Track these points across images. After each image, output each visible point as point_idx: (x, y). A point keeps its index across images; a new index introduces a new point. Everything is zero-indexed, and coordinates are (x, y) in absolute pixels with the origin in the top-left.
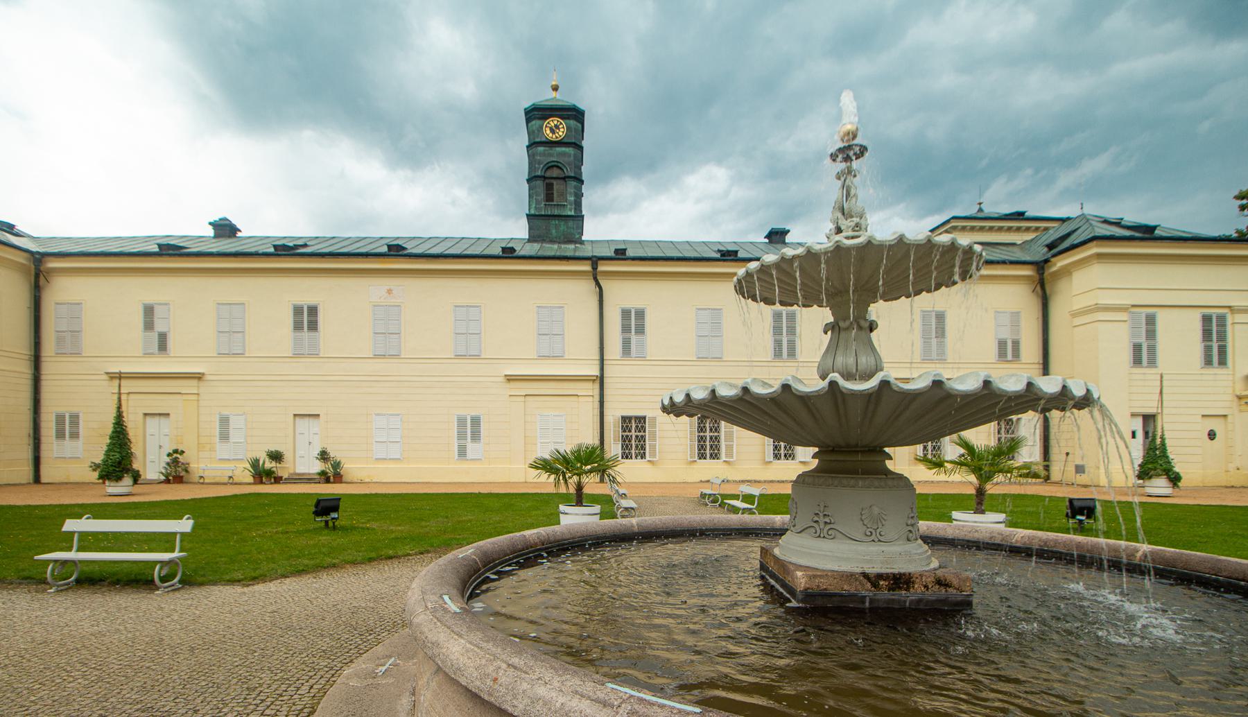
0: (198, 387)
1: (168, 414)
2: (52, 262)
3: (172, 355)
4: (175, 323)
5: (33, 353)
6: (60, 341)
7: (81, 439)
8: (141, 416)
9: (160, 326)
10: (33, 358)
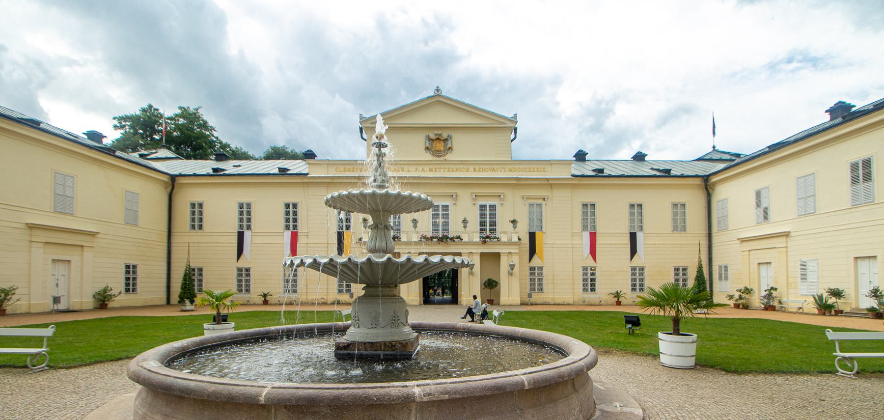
0: (787, 242)
1: (770, 263)
2: (713, 178)
3: (771, 222)
4: (772, 202)
5: (707, 232)
6: (719, 223)
7: (729, 280)
8: (756, 265)
9: (764, 205)
10: (707, 235)
